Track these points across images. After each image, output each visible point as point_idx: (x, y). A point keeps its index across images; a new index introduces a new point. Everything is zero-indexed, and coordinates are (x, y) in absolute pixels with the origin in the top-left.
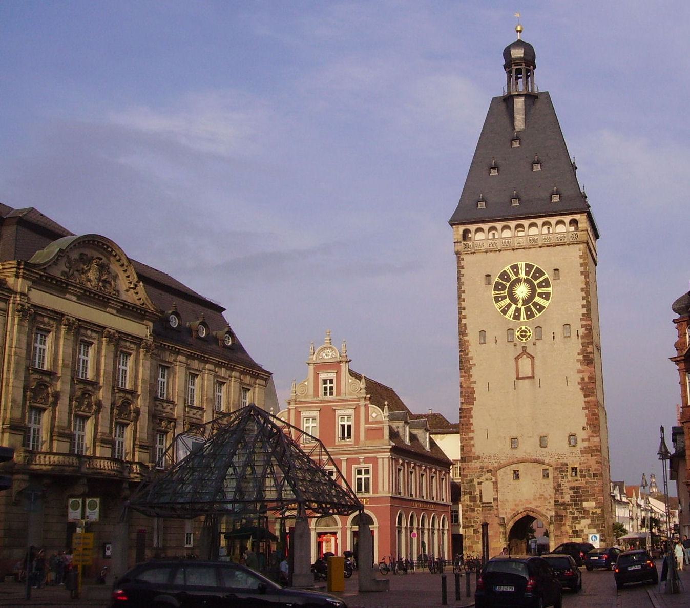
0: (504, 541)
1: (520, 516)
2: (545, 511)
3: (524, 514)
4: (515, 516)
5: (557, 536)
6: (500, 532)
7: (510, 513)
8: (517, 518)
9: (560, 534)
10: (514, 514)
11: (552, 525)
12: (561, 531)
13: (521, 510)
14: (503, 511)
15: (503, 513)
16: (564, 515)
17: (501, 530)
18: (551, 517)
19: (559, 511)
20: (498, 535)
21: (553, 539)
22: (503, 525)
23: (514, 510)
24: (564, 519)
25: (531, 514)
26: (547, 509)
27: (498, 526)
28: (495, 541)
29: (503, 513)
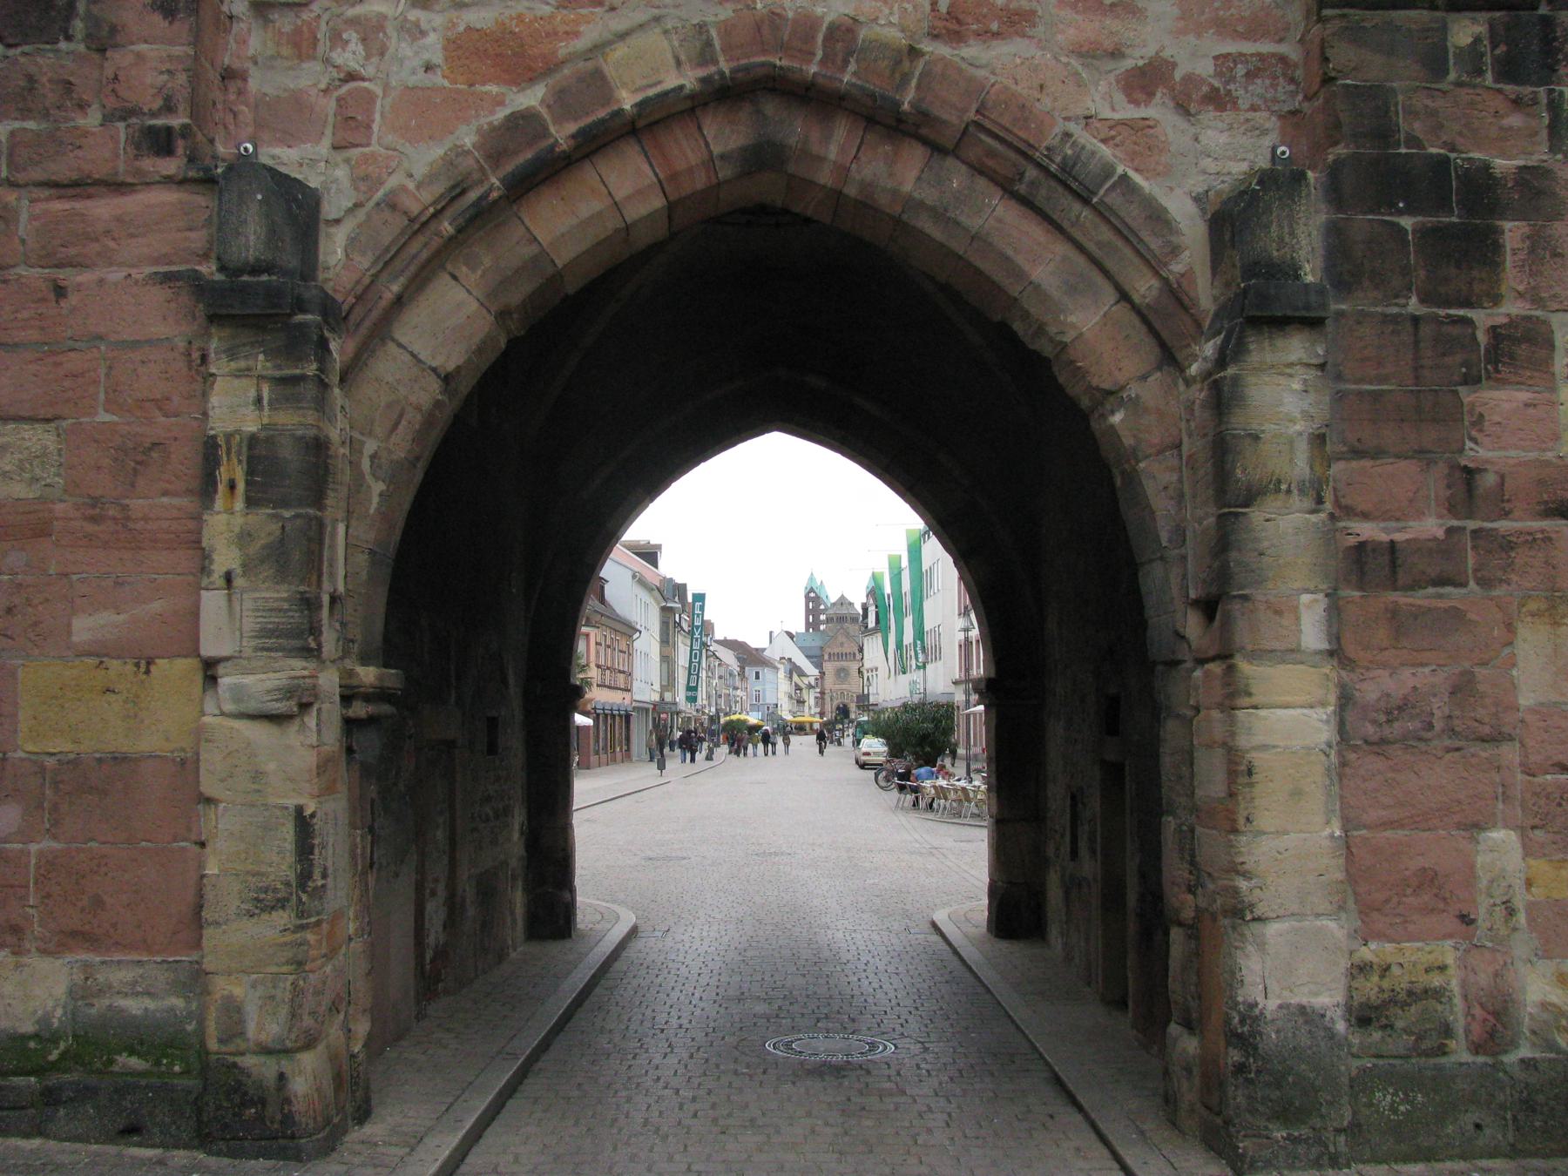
0: (299, 638)
1: (627, 189)
2: (1103, 99)
3: (724, 135)
4: (543, 173)
5: (1369, 567)
6: (210, 452)
7: (422, 110)
8: (565, 226)
9: (1431, 526)
10: (522, 123)
11: (1296, 348)
12: (1466, 486)
13: (647, 69)
14: (309, 77)
15: (290, 116)
16: (1503, 165)
17: (237, 403)
18: (1230, 220)
19: (1403, 80)
20: (157, 503)
21: (1312, 632)
22: (264, 302)
23: (524, 75)
24: (1513, 232)
25: (836, 155)
26: (1147, 80)
27: (162, 320)
28: (85, 628)
29: (290, 116)
